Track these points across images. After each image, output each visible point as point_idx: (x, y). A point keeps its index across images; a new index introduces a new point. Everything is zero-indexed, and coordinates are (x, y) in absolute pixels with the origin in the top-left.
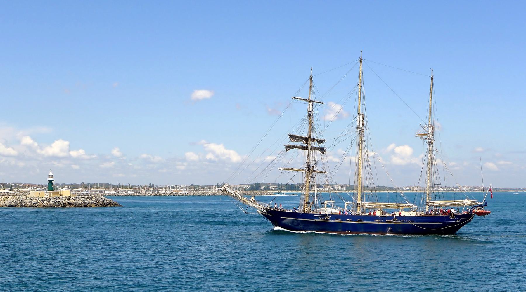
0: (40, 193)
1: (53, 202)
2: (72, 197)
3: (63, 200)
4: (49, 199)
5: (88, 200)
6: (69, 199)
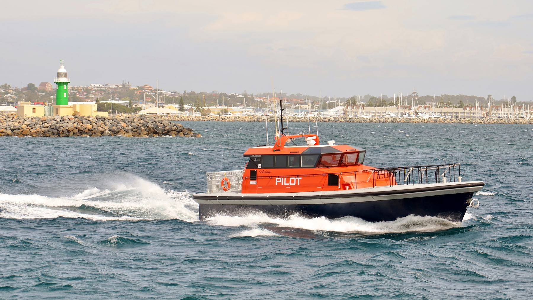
2: (89, 117)
4: (43, 122)
6: (82, 123)
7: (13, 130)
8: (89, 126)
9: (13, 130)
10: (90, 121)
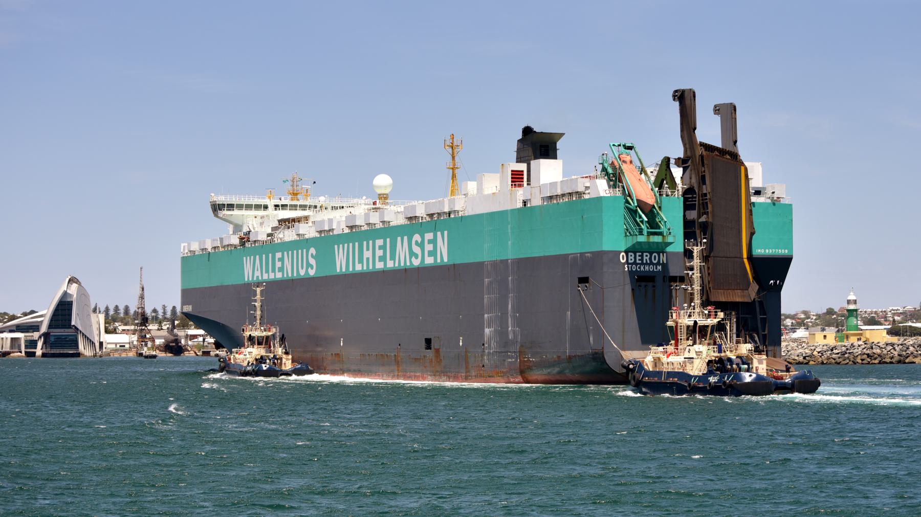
0: (825, 337)
1: (839, 355)
2: (878, 343)
3: (860, 349)
5: (911, 348)
6: (872, 349)
7: (804, 358)
8: (878, 351)
9: (804, 358)
10: (879, 346)
